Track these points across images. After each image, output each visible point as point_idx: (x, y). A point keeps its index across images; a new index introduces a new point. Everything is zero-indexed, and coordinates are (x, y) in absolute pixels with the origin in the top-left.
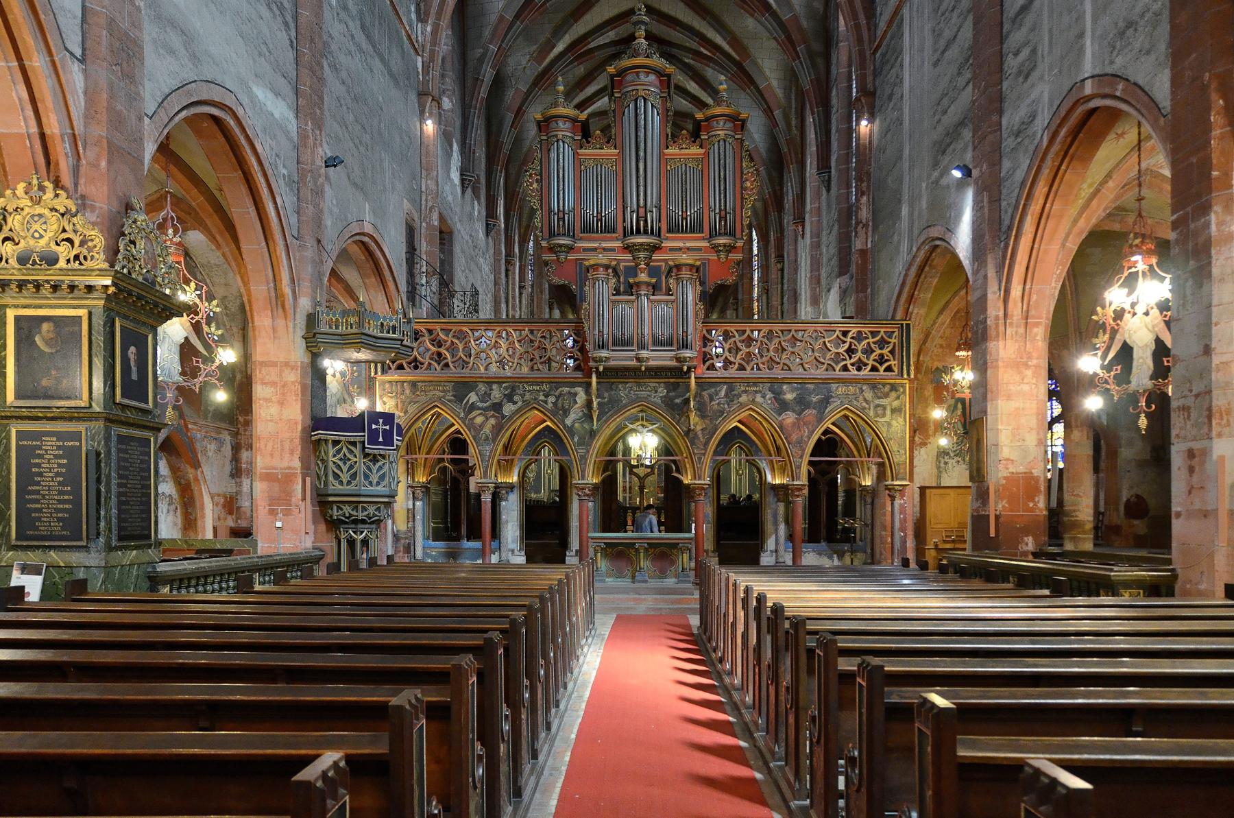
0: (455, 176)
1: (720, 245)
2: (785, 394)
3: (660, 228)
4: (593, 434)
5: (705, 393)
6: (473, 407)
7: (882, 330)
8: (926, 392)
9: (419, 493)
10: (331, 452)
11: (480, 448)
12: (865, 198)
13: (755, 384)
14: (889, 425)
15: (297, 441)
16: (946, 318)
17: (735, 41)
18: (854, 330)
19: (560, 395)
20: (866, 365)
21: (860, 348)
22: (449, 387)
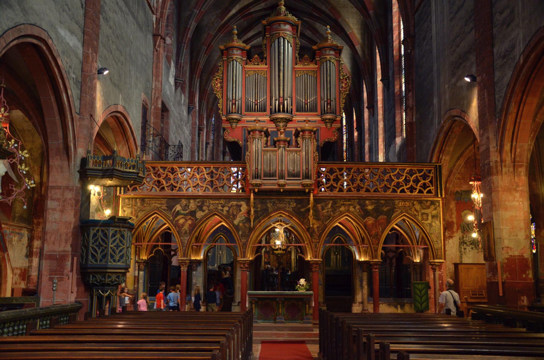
0: (172, 80)
1: (326, 119)
2: (367, 206)
3: (292, 109)
4: (251, 230)
5: (319, 206)
6: (178, 213)
7: (425, 169)
8: (451, 206)
9: (142, 266)
10: (91, 241)
11: (182, 238)
12: (411, 93)
13: (349, 200)
14: (431, 225)
15: (70, 235)
16: (461, 162)
18: (408, 169)
19: (232, 206)
21: (412, 179)
22: (164, 201)
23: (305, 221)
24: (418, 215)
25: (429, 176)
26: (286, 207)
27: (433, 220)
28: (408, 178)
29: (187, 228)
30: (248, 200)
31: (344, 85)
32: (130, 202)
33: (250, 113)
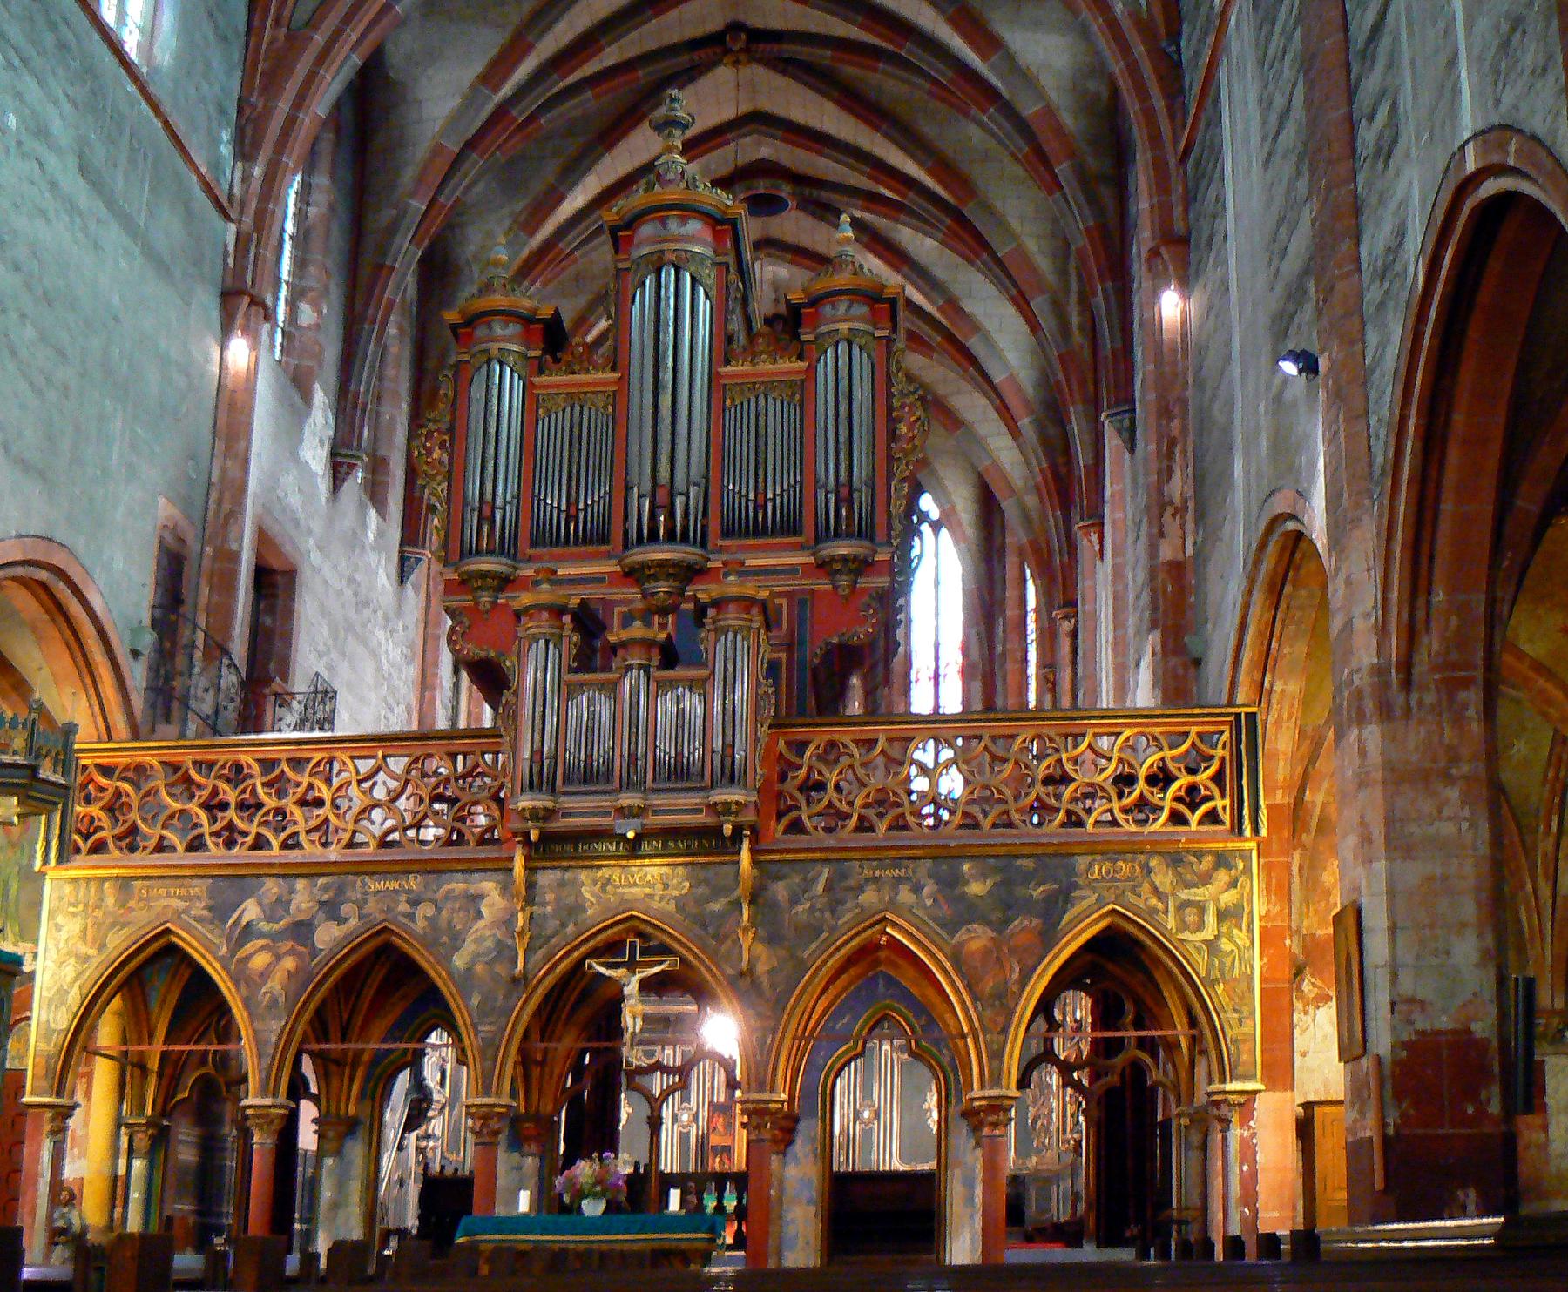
1: (833, 559)
2: (967, 883)
5: (780, 891)
7: (1194, 730)
13: (896, 862)
17: (943, 167)
21: (1142, 773)
22: (199, 888)
23: (723, 949)
24: (1166, 912)
25: (1212, 757)
27: (1224, 929)
31: (904, 430)
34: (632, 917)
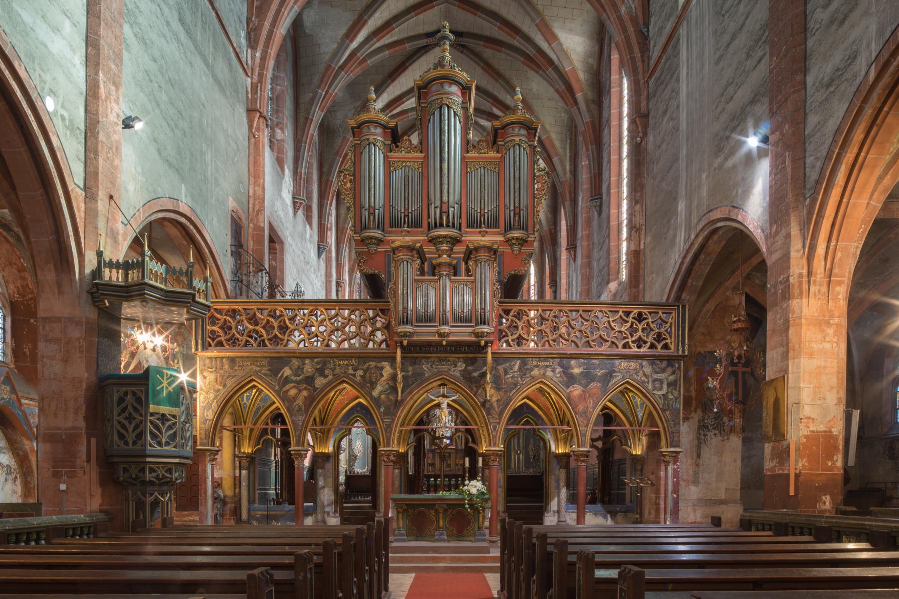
1: (513, 238)
2: (573, 369)
3: (460, 224)
4: (397, 404)
5: (501, 368)
6: (287, 380)
11: (294, 418)
13: (546, 359)
19: (368, 369)
20: (645, 343)
23: (480, 391)
26: (449, 370)
28: (635, 326)
29: (301, 403)
30: (392, 360)
32: (213, 363)
33: (396, 229)
34: (443, 378)
